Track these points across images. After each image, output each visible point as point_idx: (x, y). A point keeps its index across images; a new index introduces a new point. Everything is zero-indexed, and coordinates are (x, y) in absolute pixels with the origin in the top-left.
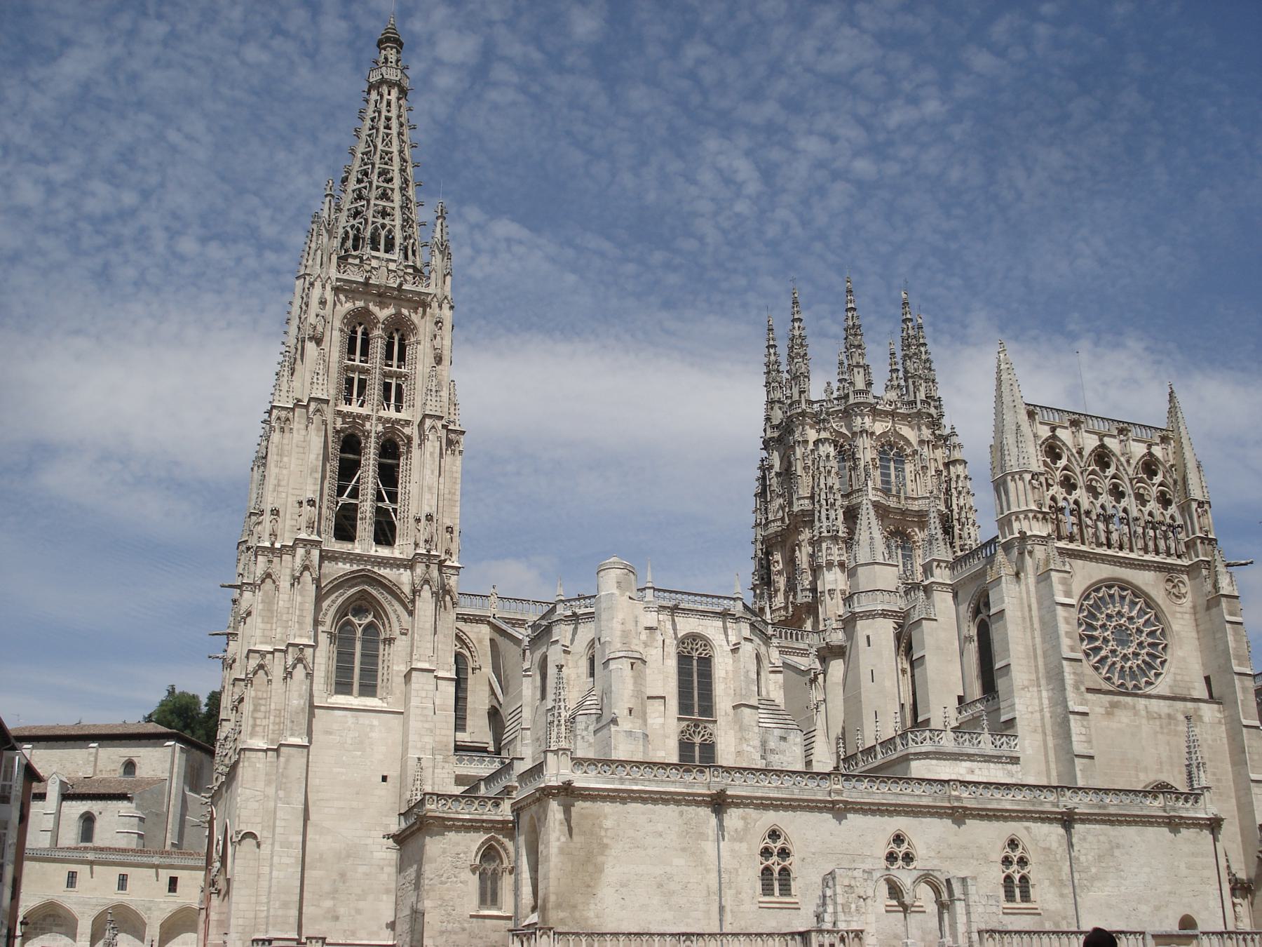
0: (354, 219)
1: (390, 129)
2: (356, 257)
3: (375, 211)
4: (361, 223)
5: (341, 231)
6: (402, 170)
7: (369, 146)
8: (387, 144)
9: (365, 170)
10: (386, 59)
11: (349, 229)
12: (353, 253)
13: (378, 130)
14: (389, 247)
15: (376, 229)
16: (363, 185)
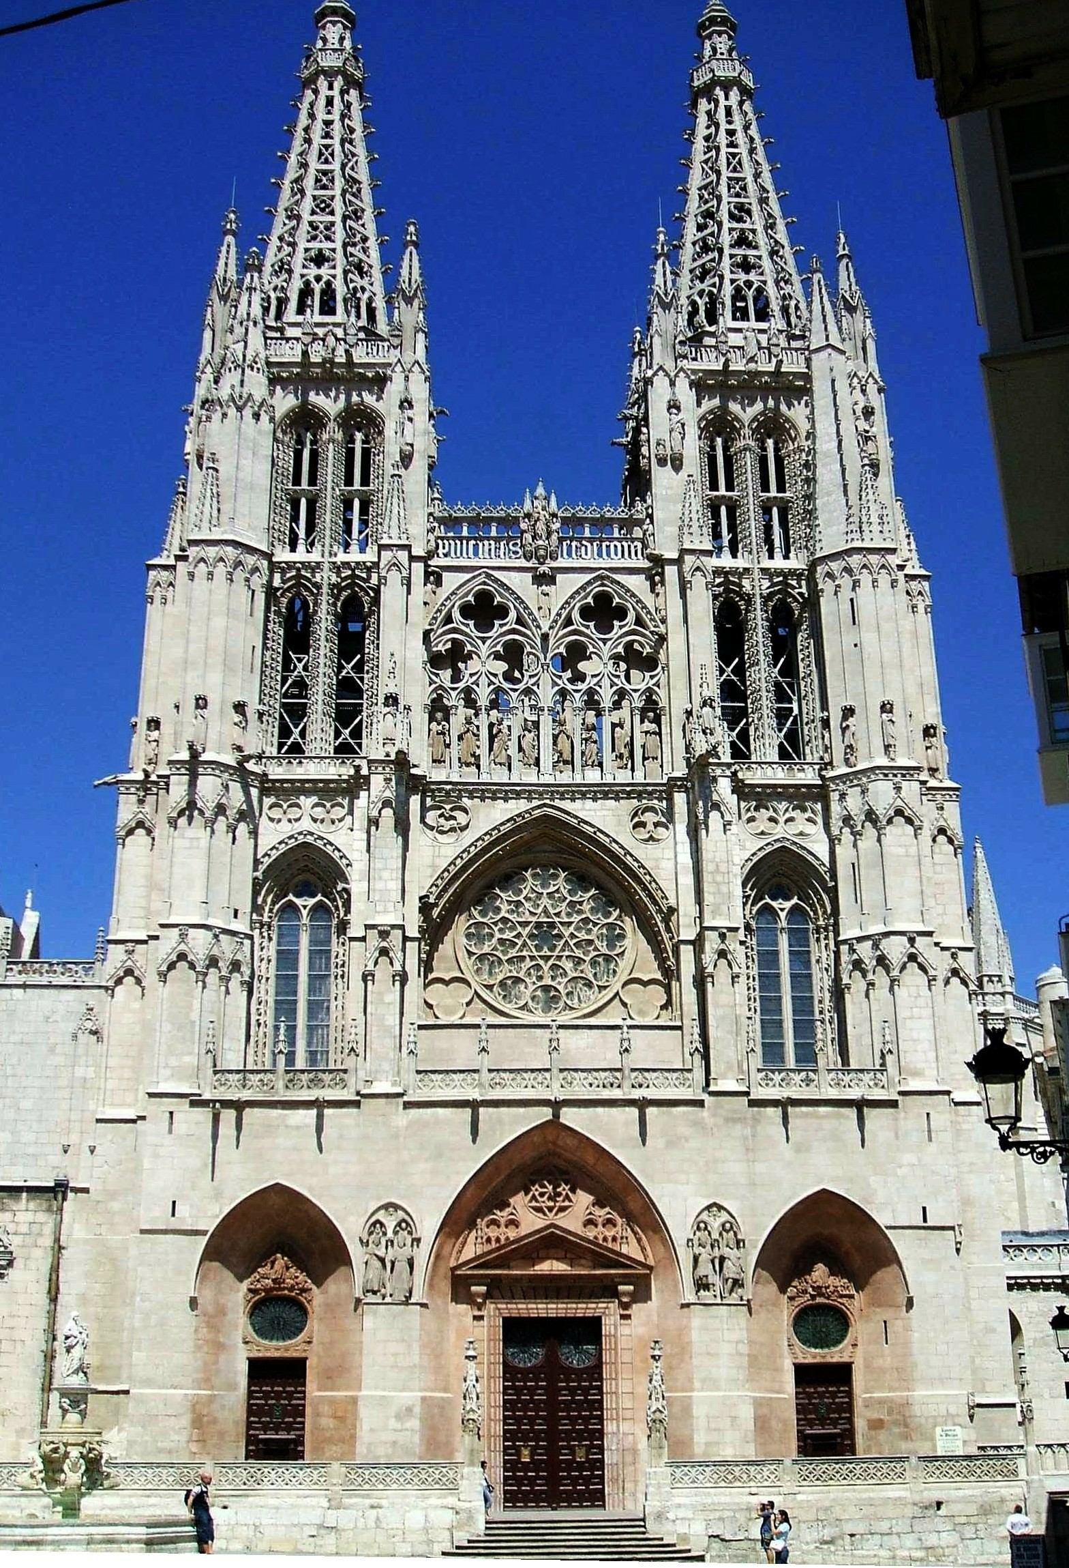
0: (702, 281)
1: (736, 146)
2: (712, 334)
3: (732, 265)
4: (714, 285)
5: (684, 301)
6: (763, 201)
8: (735, 168)
9: (707, 210)
10: (714, 50)
11: (697, 298)
12: (708, 328)
13: (718, 149)
14: (762, 315)
15: (738, 290)
16: (708, 231)
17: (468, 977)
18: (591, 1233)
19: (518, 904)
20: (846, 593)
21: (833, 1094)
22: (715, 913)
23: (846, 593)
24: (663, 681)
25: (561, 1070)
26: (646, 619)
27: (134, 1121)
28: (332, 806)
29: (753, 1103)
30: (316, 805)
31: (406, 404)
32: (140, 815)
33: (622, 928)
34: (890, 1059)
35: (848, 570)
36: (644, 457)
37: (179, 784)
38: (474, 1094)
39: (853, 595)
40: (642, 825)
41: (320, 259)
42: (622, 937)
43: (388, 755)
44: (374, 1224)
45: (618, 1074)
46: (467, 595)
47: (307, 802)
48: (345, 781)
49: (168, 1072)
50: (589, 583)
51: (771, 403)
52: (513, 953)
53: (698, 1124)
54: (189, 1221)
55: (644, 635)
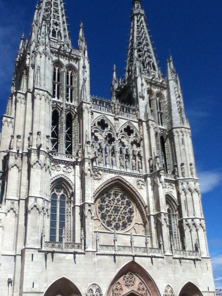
17: (100, 218)
18: (140, 292)
19: (110, 201)
20: (181, 137)
21: (189, 257)
22: (163, 209)
23: (181, 137)
25: (134, 247)
26: (138, 134)
27: (15, 256)
28: (68, 168)
29: (174, 258)
30: (64, 167)
31: (84, 67)
32: (16, 163)
33: (133, 210)
34: (199, 249)
35: (182, 132)
36: (134, 95)
37: (34, 155)
38: (113, 252)
39: (182, 138)
40: (139, 184)
41: (56, 24)
42: (133, 212)
44: (89, 290)
45: (145, 249)
46: (99, 120)
47: (62, 166)
48: (72, 162)
49: (30, 241)
50: (126, 123)
51: (159, 90)
52: (109, 213)
53: (163, 263)
54: (38, 289)
55: (137, 138)
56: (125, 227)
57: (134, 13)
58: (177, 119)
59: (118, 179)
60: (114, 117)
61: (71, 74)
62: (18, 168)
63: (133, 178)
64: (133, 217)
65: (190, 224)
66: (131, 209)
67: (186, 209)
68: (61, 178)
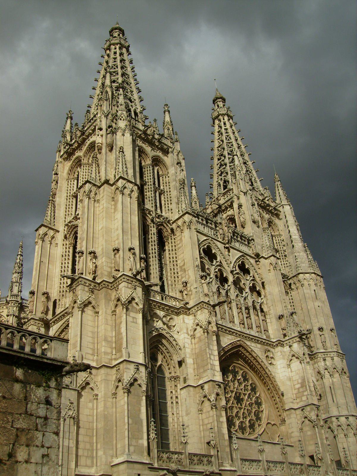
7: (228, 140)
23: (313, 287)
24: (265, 302)
26: (257, 277)
33: (261, 399)
43: (208, 302)
56: (254, 431)
57: (220, 112)
58: (304, 260)
59: (240, 346)
60: (224, 245)
61: (158, 172)
62: (94, 307)
63: (259, 346)
64: (262, 411)
65: (344, 425)
66: (257, 398)
67: (333, 401)
68: (161, 336)
